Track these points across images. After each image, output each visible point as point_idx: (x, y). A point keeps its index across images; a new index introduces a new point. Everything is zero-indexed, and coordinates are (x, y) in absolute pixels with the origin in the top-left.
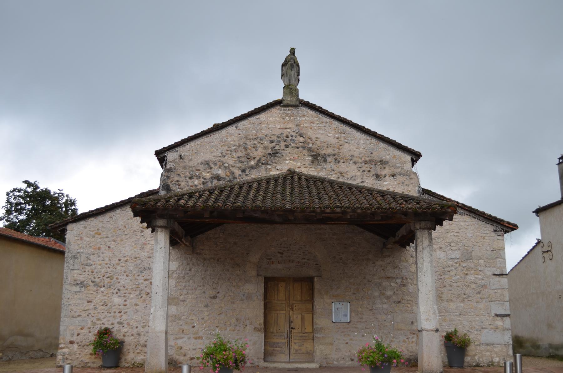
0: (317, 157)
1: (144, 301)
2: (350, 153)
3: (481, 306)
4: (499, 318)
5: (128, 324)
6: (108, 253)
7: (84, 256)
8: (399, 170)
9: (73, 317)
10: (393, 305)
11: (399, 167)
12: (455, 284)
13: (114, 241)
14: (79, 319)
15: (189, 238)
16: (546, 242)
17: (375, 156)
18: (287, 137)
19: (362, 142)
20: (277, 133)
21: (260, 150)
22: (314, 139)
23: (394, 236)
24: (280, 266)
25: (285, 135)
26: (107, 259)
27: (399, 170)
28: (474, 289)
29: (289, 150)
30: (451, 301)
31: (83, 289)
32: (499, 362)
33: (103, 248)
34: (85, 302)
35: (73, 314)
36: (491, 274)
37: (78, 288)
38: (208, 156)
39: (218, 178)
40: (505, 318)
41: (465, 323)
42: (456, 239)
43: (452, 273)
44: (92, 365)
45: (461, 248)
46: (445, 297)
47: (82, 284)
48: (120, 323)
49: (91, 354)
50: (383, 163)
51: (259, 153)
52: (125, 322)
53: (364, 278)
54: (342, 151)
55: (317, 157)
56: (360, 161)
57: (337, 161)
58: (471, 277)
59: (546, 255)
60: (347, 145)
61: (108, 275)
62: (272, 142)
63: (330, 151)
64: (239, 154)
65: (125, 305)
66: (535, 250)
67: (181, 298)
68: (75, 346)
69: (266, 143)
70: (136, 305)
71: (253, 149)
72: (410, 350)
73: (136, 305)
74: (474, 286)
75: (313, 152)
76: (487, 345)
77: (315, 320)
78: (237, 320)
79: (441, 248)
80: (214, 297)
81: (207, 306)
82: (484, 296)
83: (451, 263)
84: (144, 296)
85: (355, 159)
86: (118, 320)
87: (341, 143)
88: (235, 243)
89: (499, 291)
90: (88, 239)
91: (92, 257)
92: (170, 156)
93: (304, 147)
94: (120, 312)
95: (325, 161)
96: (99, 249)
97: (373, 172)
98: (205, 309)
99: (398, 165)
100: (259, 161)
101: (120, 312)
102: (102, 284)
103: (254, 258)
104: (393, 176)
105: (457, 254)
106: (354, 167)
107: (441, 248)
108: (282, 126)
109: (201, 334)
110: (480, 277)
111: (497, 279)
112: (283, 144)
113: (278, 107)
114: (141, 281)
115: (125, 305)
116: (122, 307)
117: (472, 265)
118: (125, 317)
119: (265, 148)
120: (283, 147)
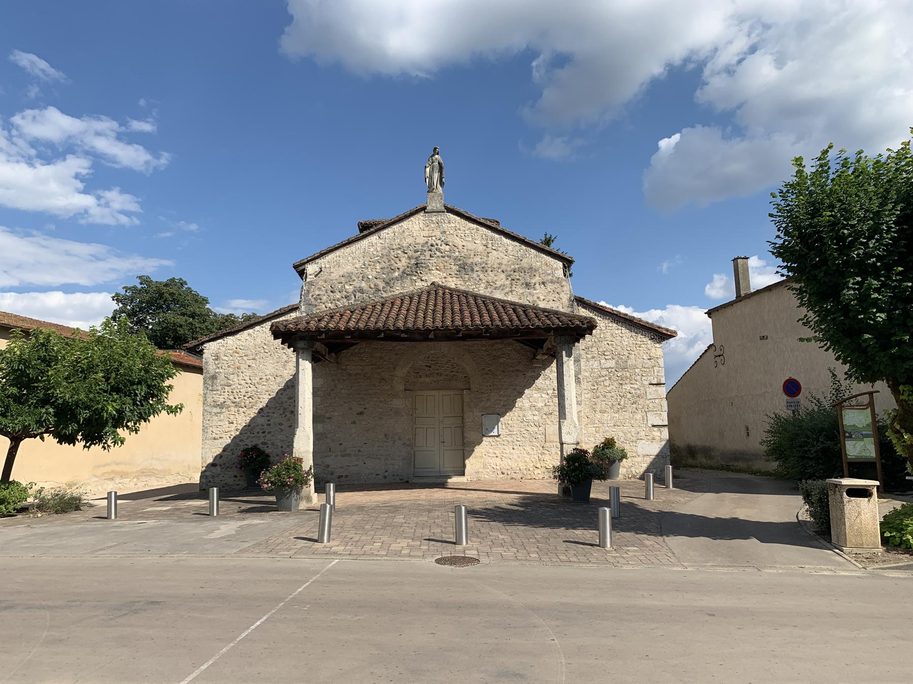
0: (464, 268)
1: (289, 420)
2: (498, 261)
4: (655, 429)
5: (273, 444)
6: (248, 373)
8: (550, 277)
9: (215, 439)
10: (545, 417)
13: (254, 359)
14: (220, 440)
15: (333, 354)
16: (718, 347)
17: (525, 263)
18: (432, 245)
19: (510, 248)
20: (421, 240)
21: (403, 260)
22: (460, 247)
23: (542, 348)
24: (428, 380)
25: (429, 244)
26: (247, 378)
27: (550, 277)
28: (629, 399)
29: (434, 260)
30: (605, 412)
31: (224, 410)
33: (243, 367)
34: (227, 423)
35: (214, 435)
36: (647, 383)
37: (218, 410)
38: (349, 268)
39: (361, 291)
40: (662, 429)
41: (621, 434)
43: (607, 383)
44: (237, 488)
46: (598, 408)
47: (222, 406)
48: (263, 443)
49: (235, 476)
50: (532, 270)
51: (403, 263)
52: (270, 442)
53: (514, 389)
54: (490, 258)
55: (464, 268)
56: (509, 269)
57: (484, 270)
58: (628, 387)
59: (718, 359)
61: (250, 394)
62: (416, 251)
63: (477, 259)
64: (383, 265)
65: (269, 425)
66: (707, 353)
67: (327, 415)
68: (218, 468)
69: (410, 253)
70: (281, 424)
71: (397, 260)
73: (281, 424)
74: (629, 396)
75: (460, 260)
76: (644, 456)
77: (466, 434)
78: (386, 435)
79: (593, 357)
80: (361, 413)
81: (354, 423)
83: (604, 373)
84: (289, 415)
85: (503, 267)
86: (262, 440)
87: (489, 250)
88: (381, 358)
89: (657, 401)
90: (225, 358)
91: (232, 376)
92: (311, 269)
93: (449, 257)
94: (264, 432)
95: (472, 270)
98: (353, 426)
99: (549, 272)
100: (404, 272)
101: (264, 432)
102: (243, 404)
103: (401, 372)
104: (543, 283)
105: (612, 364)
106: (503, 276)
107: (593, 357)
108: (426, 233)
109: (348, 452)
111: (654, 388)
112: (428, 254)
113: (422, 213)
114: (285, 400)
115: (269, 425)
116: (265, 427)
117: (628, 374)
118: (269, 436)
119: (409, 258)
120: (428, 257)
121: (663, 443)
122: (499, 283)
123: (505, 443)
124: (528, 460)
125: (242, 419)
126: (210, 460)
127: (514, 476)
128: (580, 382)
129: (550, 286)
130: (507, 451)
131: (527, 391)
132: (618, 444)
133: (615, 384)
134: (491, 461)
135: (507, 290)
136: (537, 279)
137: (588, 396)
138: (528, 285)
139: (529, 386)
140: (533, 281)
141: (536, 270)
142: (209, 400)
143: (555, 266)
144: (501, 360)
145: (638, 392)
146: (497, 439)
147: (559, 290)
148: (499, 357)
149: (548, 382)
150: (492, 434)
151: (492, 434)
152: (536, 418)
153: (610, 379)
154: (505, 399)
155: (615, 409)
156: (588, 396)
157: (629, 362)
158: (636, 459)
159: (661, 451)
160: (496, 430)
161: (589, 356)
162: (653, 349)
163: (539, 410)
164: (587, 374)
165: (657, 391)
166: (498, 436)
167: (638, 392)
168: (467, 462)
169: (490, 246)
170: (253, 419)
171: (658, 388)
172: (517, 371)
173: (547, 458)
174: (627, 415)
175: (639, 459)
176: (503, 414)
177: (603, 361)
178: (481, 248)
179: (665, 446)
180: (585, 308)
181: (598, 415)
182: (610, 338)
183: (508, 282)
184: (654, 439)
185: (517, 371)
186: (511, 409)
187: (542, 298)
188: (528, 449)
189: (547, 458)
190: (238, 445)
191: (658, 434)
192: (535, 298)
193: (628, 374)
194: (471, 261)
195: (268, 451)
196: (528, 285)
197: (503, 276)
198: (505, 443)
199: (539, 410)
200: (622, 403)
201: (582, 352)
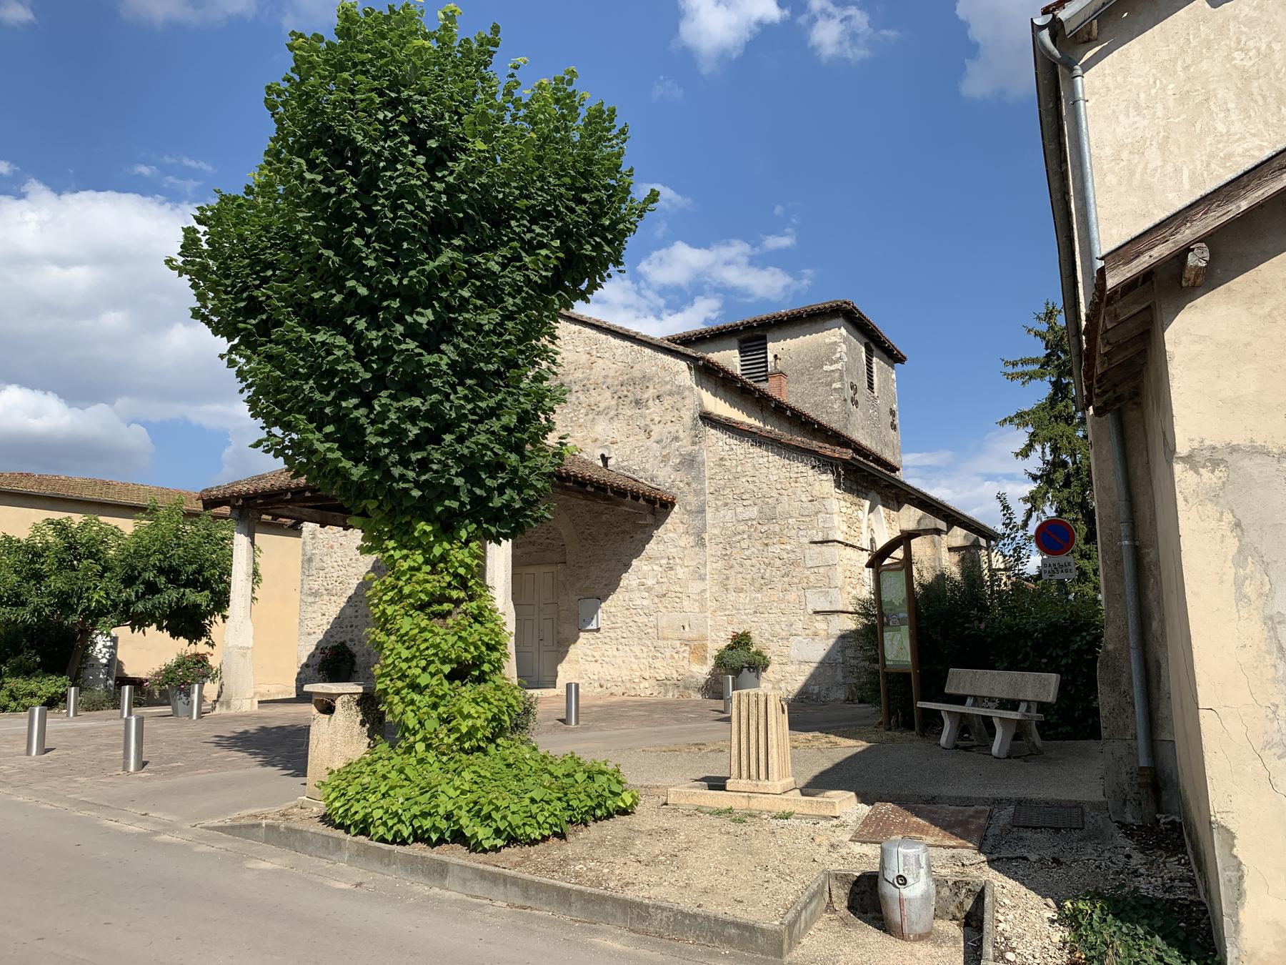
2: (603, 373)
3: (792, 596)
4: (819, 617)
7: (318, 557)
8: (669, 387)
10: (656, 600)
11: (667, 383)
12: (748, 562)
19: (619, 352)
27: (669, 387)
30: (741, 590)
32: (818, 694)
33: (336, 545)
36: (806, 541)
37: (311, 599)
42: (751, 486)
45: (759, 501)
46: (731, 584)
47: (316, 594)
48: (352, 640)
50: (645, 379)
53: (619, 561)
57: (585, 389)
60: (600, 361)
72: (681, 671)
74: (778, 562)
79: (726, 504)
82: (796, 580)
83: (741, 528)
85: (609, 381)
87: (593, 359)
89: (821, 570)
96: (332, 547)
97: (631, 398)
105: (753, 512)
107: (726, 504)
110: (788, 547)
111: (817, 548)
117: (777, 528)
121: (832, 641)
122: (602, 406)
123: (608, 640)
124: (635, 667)
125: (333, 611)
126: (304, 660)
127: (614, 690)
128: (704, 545)
129: (668, 401)
130: (610, 653)
131: (635, 562)
132: (757, 642)
133: (758, 545)
134: (587, 667)
135: (613, 413)
136: (651, 392)
137: (719, 565)
138: (637, 402)
139: (637, 553)
140: (646, 396)
141: (650, 379)
142: (306, 587)
143: (676, 369)
144: (604, 518)
145: (792, 556)
146: (598, 635)
147: (679, 405)
148: (602, 513)
149: (661, 547)
150: (590, 627)
151: (590, 627)
152: (645, 602)
153: (749, 537)
154: (607, 575)
155: (757, 585)
156: (719, 565)
157: (779, 507)
158: (787, 668)
159: (828, 656)
160: (594, 621)
161: (719, 503)
162: (817, 484)
163: (649, 590)
164: (716, 531)
165: (821, 553)
166: (598, 630)
167: (792, 556)
168: (559, 667)
169: (594, 353)
170: (342, 609)
171: (824, 548)
172: (623, 532)
173: (658, 663)
174: (777, 594)
175: (792, 668)
176: (602, 598)
177: (740, 509)
178: (584, 358)
179: (833, 646)
180: (713, 427)
181: (732, 596)
182: (751, 471)
183: (614, 402)
184: (816, 634)
185: (623, 532)
186: (614, 590)
187: (657, 419)
188: (637, 649)
189: (658, 663)
190: (328, 642)
191: (824, 626)
192: (648, 421)
193: (777, 528)
194: (570, 377)
195: (355, 649)
196: (637, 402)
197: (608, 394)
198: (608, 640)
199: (649, 590)
200: (767, 576)
201: (709, 497)
